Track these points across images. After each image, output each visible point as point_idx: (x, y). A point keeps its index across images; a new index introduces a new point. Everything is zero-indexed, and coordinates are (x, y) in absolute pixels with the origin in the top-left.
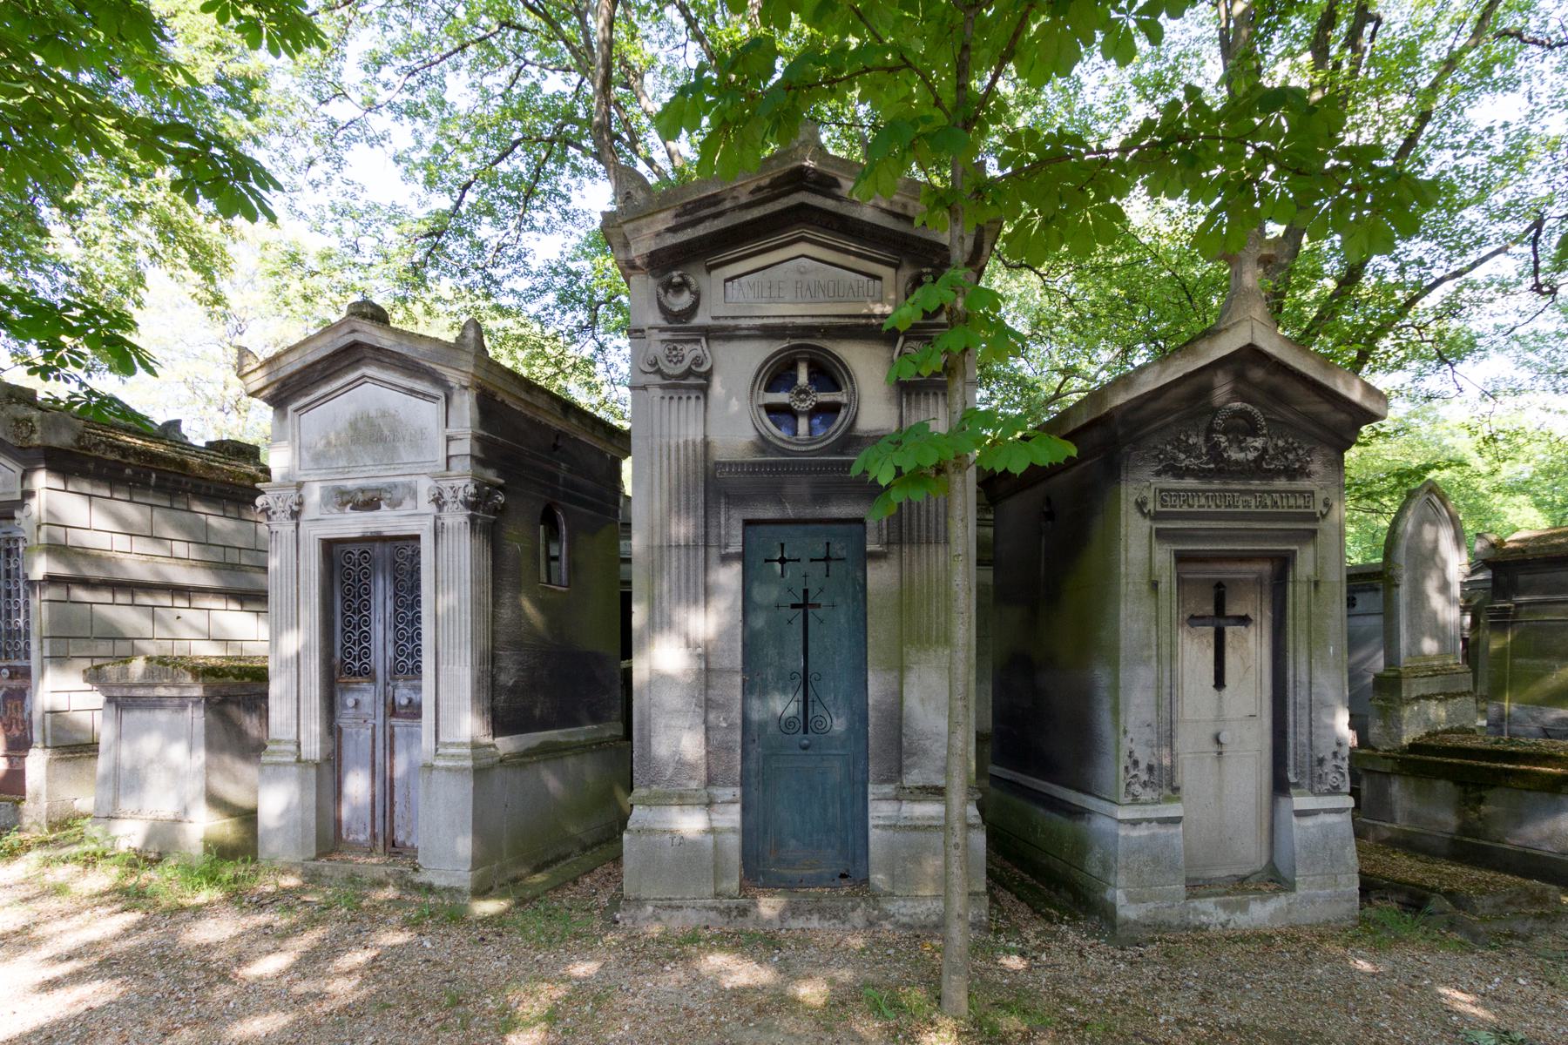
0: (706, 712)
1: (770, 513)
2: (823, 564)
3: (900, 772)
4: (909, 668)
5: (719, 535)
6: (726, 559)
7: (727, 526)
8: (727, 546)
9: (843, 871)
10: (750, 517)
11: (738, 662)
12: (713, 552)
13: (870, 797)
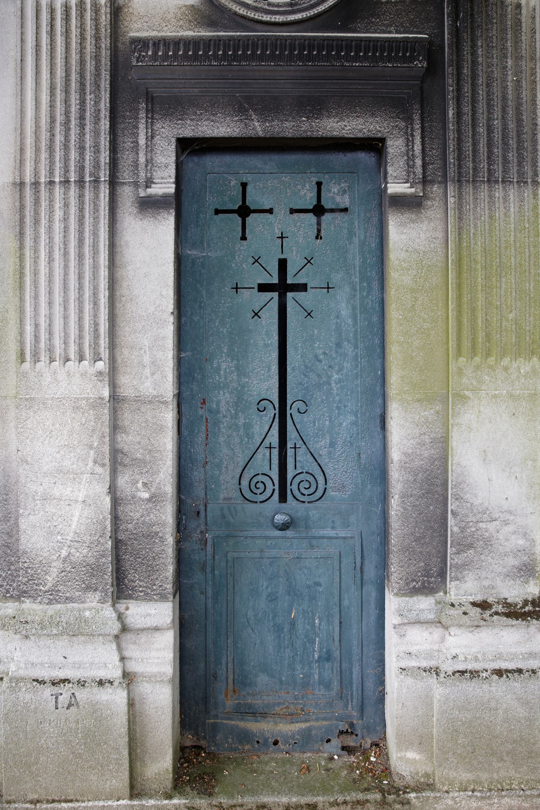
0: (114, 473)
1: (221, 127)
2: (311, 218)
3: (442, 574)
4: (462, 398)
5: (136, 165)
6: (149, 205)
7: (150, 148)
8: (149, 183)
9: (343, 726)
10: (188, 133)
11: (168, 387)
12: (126, 193)
13: (391, 619)
